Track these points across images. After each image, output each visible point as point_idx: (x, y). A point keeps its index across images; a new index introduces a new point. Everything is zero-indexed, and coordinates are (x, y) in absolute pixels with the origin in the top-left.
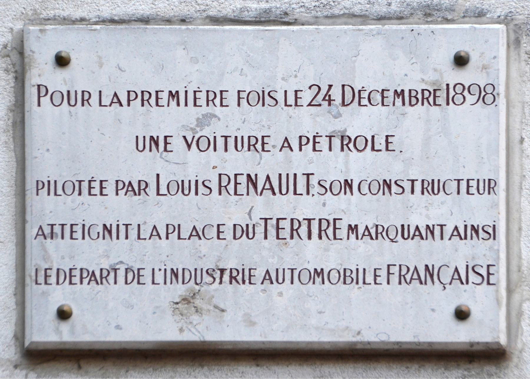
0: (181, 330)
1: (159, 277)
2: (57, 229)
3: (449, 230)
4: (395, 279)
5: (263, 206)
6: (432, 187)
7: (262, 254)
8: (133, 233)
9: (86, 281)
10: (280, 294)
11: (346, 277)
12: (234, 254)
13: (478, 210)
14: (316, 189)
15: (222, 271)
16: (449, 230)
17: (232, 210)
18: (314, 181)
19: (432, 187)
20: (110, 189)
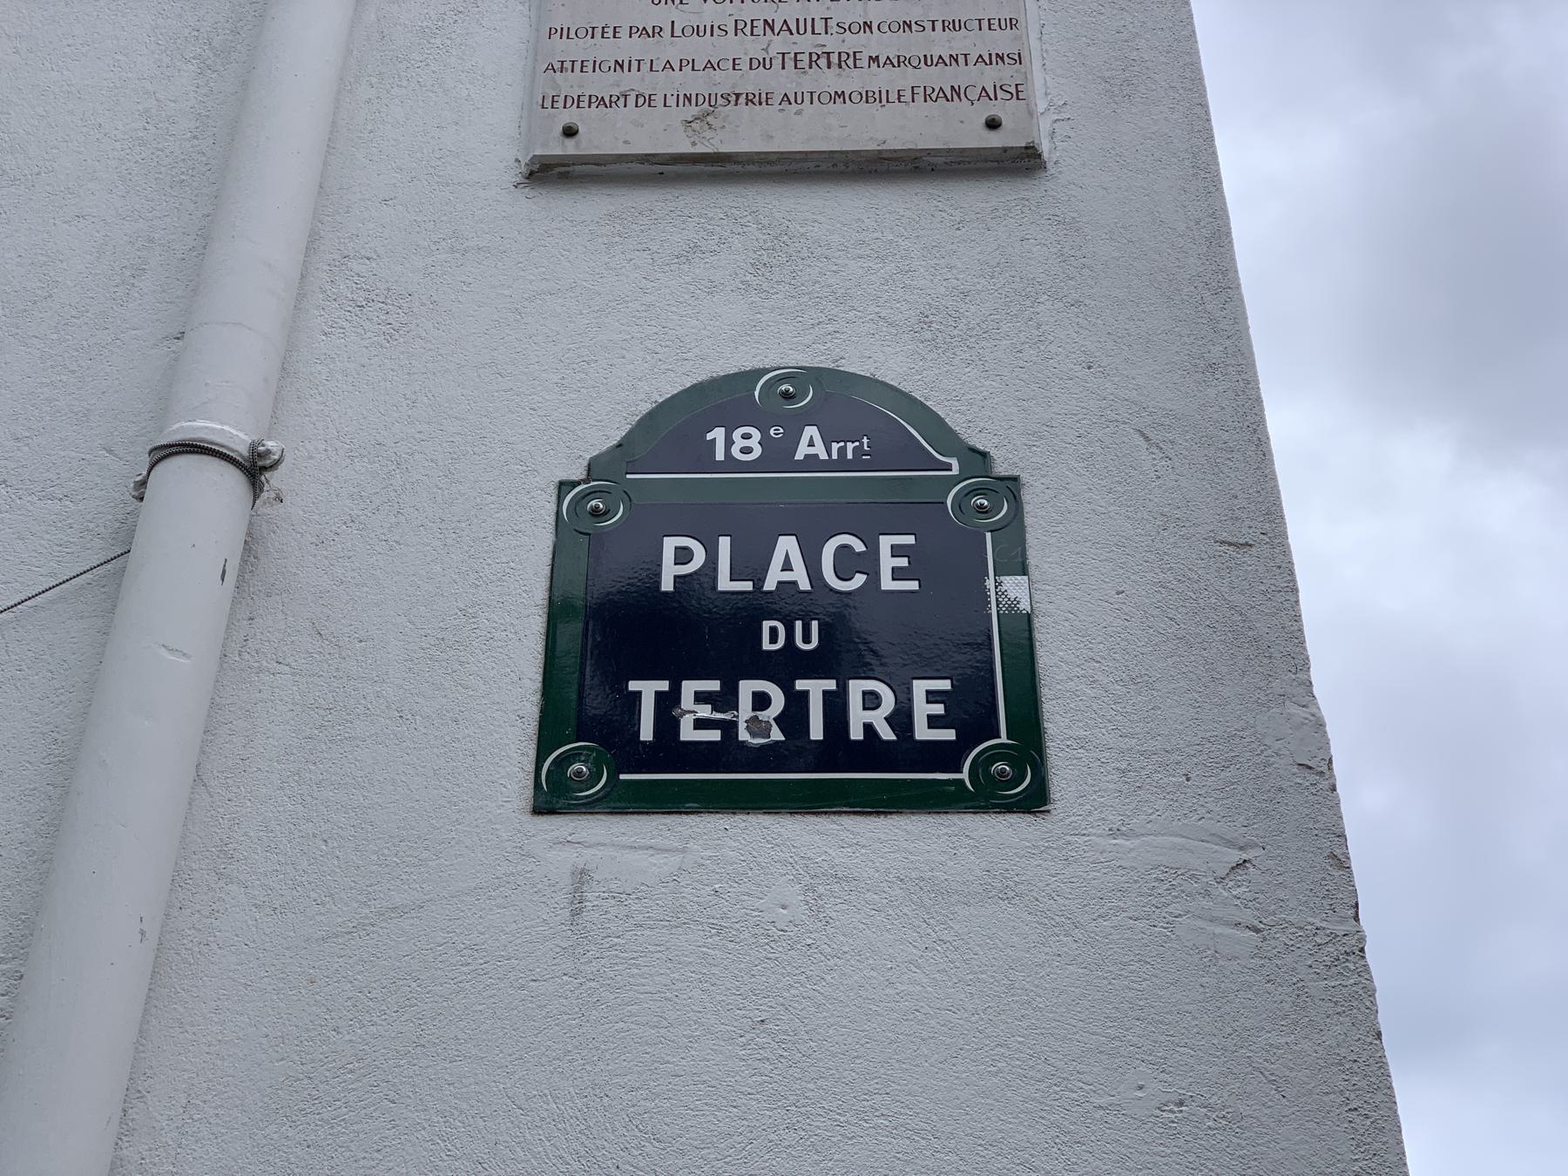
0: (694, 144)
1: (671, 101)
2: (568, 65)
3: (972, 59)
4: (920, 98)
5: (779, 43)
6: (953, 26)
7: (781, 81)
8: (645, 67)
9: (594, 106)
10: (798, 113)
11: (867, 97)
12: (752, 82)
13: (1001, 42)
14: (834, 29)
15: (738, 96)
16: (972, 59)
17: (752, 47)
18: (831, 23)
19: (953, 26)
20: (623, 33)
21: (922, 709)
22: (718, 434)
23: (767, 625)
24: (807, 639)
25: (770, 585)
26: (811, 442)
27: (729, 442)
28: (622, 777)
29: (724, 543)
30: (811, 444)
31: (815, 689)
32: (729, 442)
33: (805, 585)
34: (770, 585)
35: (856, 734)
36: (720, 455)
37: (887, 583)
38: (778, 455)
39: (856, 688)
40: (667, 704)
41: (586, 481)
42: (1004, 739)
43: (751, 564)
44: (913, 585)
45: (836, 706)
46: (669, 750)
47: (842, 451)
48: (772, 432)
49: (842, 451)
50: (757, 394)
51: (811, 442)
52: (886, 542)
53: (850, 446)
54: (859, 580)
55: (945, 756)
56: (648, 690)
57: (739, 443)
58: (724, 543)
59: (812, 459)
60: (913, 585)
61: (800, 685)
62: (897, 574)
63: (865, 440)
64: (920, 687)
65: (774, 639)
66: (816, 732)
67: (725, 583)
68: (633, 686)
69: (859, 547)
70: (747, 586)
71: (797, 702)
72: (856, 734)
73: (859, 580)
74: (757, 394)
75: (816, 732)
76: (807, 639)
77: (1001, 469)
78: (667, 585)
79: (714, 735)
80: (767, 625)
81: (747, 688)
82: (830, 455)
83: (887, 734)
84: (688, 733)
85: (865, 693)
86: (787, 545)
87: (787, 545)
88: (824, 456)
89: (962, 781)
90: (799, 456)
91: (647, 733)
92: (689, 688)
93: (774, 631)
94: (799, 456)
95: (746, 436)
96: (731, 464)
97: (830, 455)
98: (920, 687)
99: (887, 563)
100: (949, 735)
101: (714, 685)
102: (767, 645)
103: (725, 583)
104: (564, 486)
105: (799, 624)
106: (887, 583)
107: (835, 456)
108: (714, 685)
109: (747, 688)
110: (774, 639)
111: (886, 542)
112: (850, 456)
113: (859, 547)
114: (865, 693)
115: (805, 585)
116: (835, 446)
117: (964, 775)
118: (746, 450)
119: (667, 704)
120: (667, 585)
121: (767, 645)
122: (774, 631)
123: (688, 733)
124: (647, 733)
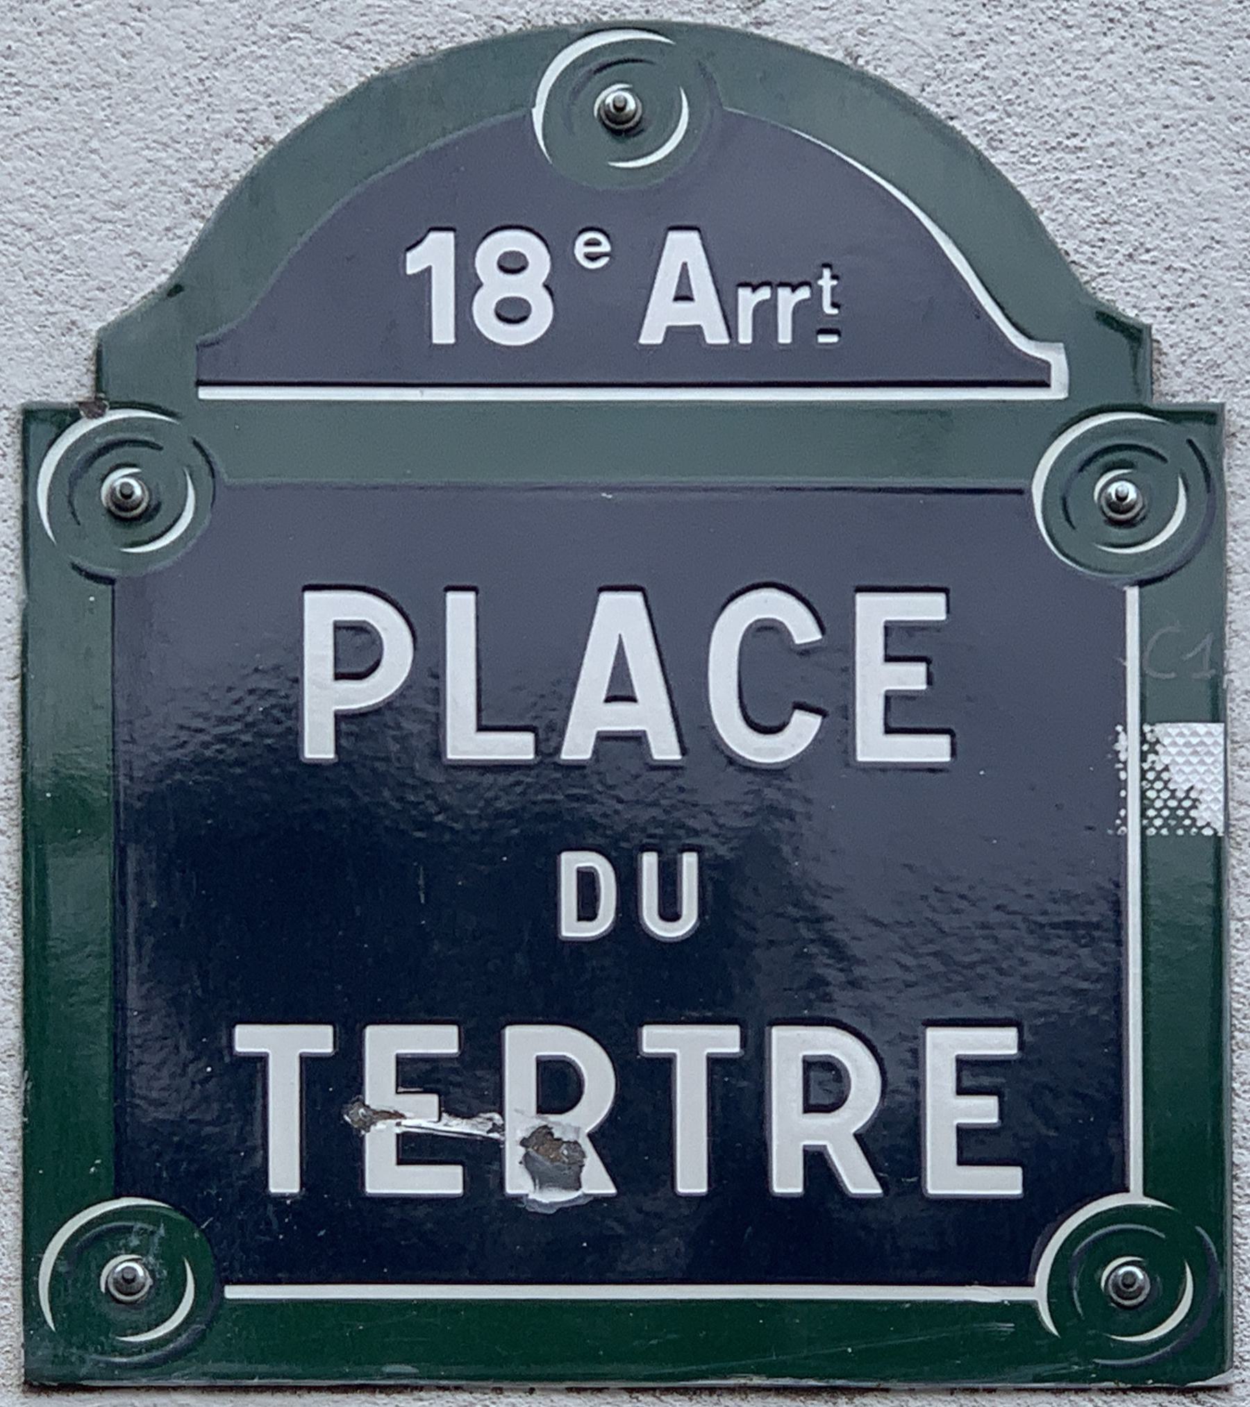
21: (948, 1111)
22: (434, 254)
23: (571, 863)
24: (669, 911)
25: (577, 746)
26: (683, 293)
27: (467, 285)
28: (233, 1292)
29: (461, 610)
30: (684, 295)
31: (690, 1048)
32: (467, 285)
33: (665, 748)
34: (577, 746)
35: (787, 1179)
36: (443, 332)
37: (874, 744)
38: (595, 329)
39: (791, 1047)
40: (332, 1086)
41: (94, 407)
42: (1135, 1196)
43: (529, 686)
44: (933, 749)
45: (738, 1095)
46: (339, 1223)
47: (765, 315)
48: (580, 250)
49: (765, 315)
50: (538, 114)
51: (683, 293)
52: (874, 613)
53: (787, 300)
54: (804, 729)
55: (988, 1240)
56: (284, 1049)
57: (496, 287)
58: (461, 610)
59: (684, 338)
60: (933, 749)
61: (655, 1039)
62: (902, 715)
63: (826, 282)
64: (945, 1047)
65: (587, 910)
66: (692, 1175)
67: (465, 742)
68: (248, 1039)
69: (803, 628)
70: (517, 747)
71: (646, 1084)
72: (787, 1179)
73: (804, 729)
74: (538, 114)
75: (692, 1175)
76: (669, 911)
77: (1178, 385)
78: (318, 744)
79: (444, 1181)
80: (571, 863)
81: (525, 1046)
82: (732, 330)
83: (859, 1180)
84: (385, 1175)
85: (809, 1065)
86: (620, 621)
87: (620, 621)
88: (716, 335)
89: (1029, 1309)
90: (652, 335)
91: (284, 1176)
92: (385, 1045)
93: (587, 880)
94: (652, 335)
95: (512, 265)
96: (474, 359)
97: (732, 330)
98: (945, 1047)
99: (877, 678)
100: (1005, 1182)
101: (442, 1040)
102: (571, 928)
103: (465, 742)
104: (39, 423)
105: (649, 862)
106: (874, 744)
107: (745, 336)
108: (442, 1040)
109: (525, 1046)
110: (587, 910)
111: (874, 613)
112: (785, 336)
113: (803, 628)
114: (809, 1065)
115: (665, 748)
116: (748, 300)
117: (1037, 1293)
118: (513, 312)
119: (332, 1086)
120: (318, 744)
121: (571, 928)
122: (587, 880)
123: (385, 1175)
124: (284, 1176)
